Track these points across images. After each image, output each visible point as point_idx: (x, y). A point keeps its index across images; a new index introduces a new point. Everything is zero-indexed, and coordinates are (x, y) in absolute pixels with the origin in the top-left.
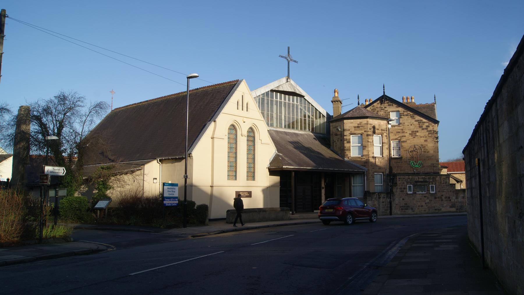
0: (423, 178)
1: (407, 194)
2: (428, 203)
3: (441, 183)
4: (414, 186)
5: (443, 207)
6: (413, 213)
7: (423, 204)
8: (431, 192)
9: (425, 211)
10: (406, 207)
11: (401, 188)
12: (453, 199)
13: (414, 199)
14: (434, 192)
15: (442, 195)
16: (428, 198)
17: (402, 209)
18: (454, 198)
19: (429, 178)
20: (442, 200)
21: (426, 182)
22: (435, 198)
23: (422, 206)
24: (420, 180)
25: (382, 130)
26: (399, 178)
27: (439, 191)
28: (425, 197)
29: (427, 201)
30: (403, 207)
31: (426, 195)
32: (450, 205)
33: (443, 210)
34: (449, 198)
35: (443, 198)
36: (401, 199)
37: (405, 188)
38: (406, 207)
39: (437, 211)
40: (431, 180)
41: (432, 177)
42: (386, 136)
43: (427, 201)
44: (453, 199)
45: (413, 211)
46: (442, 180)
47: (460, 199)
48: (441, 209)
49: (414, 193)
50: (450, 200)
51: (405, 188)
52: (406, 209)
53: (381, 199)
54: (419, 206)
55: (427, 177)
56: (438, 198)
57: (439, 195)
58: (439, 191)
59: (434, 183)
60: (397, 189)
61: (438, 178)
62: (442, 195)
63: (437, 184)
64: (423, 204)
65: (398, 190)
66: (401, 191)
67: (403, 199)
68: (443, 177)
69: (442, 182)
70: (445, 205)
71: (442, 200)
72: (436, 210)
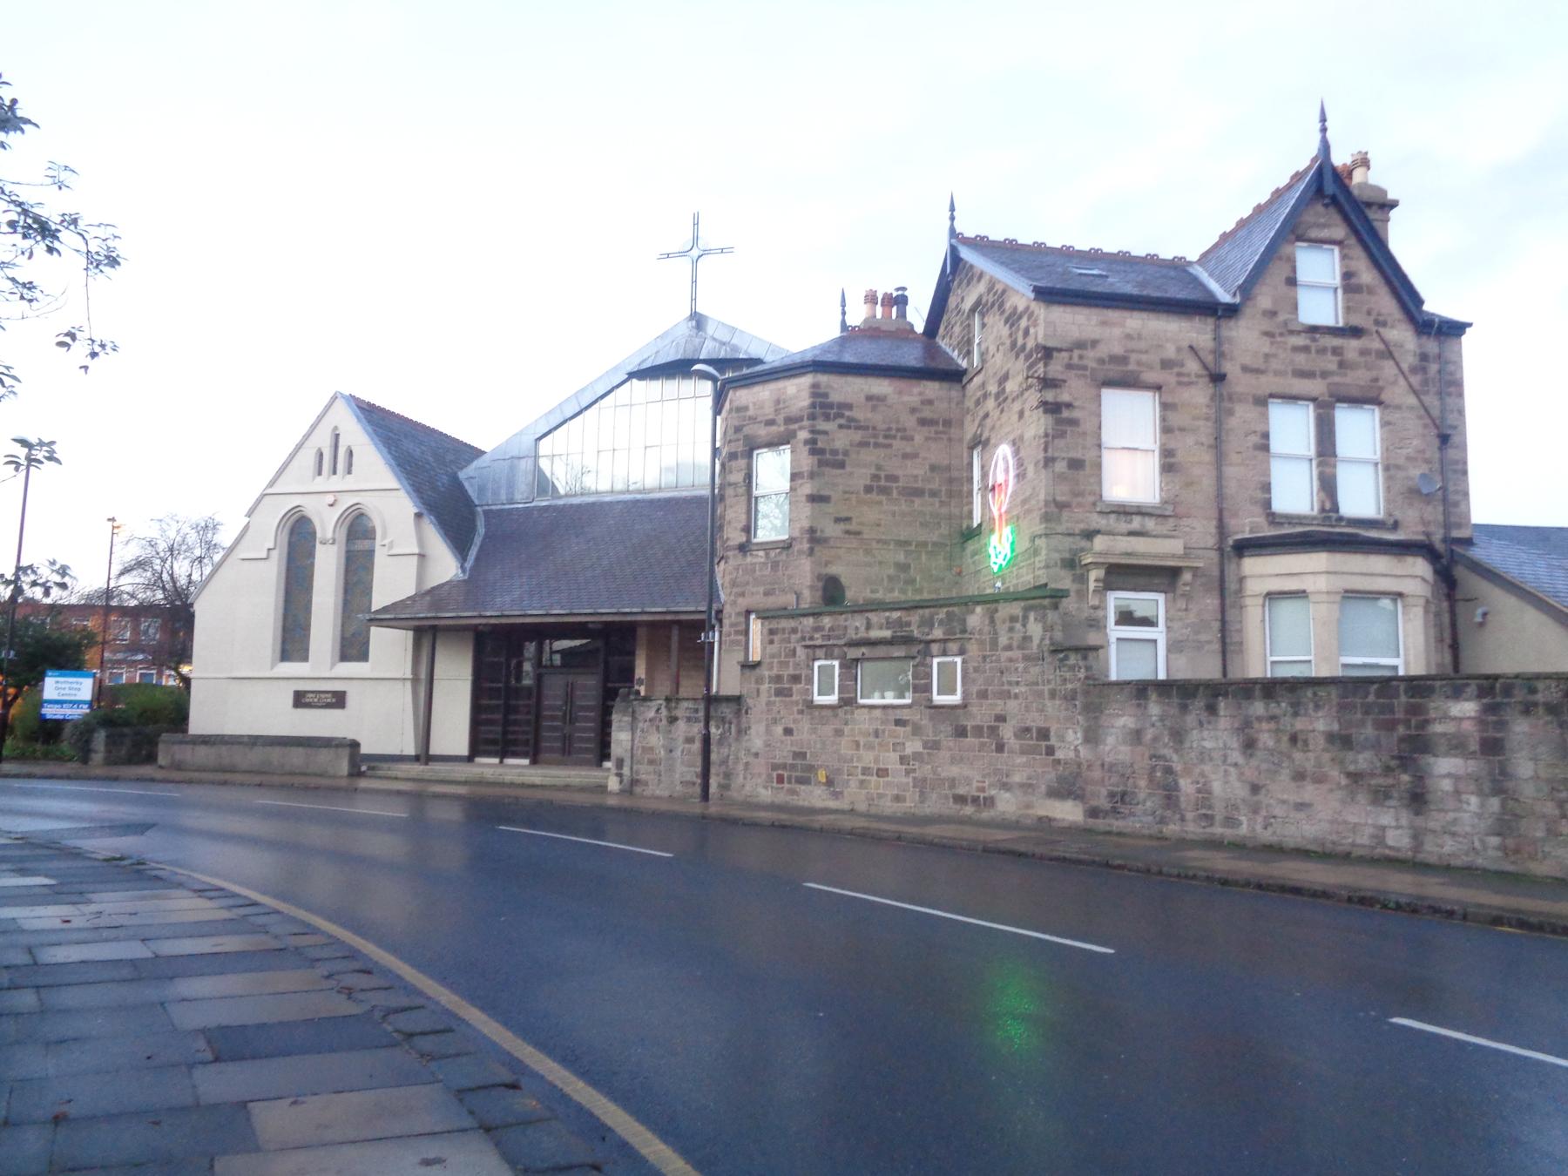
0: (889, 624)
1: (810, 705)
2: (917, 756)
3: (994, 643)
4: (849, 666)
5: (1006, 787)
6: (832, 804)
7: (891, 760)
8: (938, 699)
9: (897, 798)
10: (798, 770)
11: (778, 679)
12: (1070, 742)
13: (839, 733)
14: (955, 699)
15: (1001, 718)
16: (917, 730)
17: (780, 779)
18: (1074, 736)
19: (928, 623)
20: (1000, 748)
21: (908, 640)
22: (961, 732)
23: (882, 773)
24: (875, 634)
25: (789, 420)
26: (772, 632)
27: (983, 695)
28: (898, 722)
29: (913, 746)
30: (784, 767)
31: (904, 715)
32: (1051, 776)
33: (1007, 804)
34: (1044, 734)
35: (1007, 732)
36: (779, 730)
37: (796, 679)
38: (798, 770)
39: (969, 810)
40: (938, 633)
41: (942, 614)
42: (806, 442)
43: (913, 746)
44: (1070, 742)
45: (837, 795)
46: (1002, 630)
47: (1114, 746)
48: (990, 802)
49: (847, 702)
50: (1050, 751)
51: (796, 679)
52: (801, 781)
53: (681, 725)
54: (866, 771)
55: (915, 618)
56: (978, 731)
57: (981, 714)
58: (983, 695)
59: (953, 647)
60: (759, 681)
61: (976, 618)
62: (1001, 718)
63: (973, 649)
64: (891, 760)
65: (765, 687)
66: (779, 693)
67: (788, 731)
68: (1005, 610)
69: (1003, 640)
70: (1017, 778)
71: (1000, 748)
72: (960, 799)
